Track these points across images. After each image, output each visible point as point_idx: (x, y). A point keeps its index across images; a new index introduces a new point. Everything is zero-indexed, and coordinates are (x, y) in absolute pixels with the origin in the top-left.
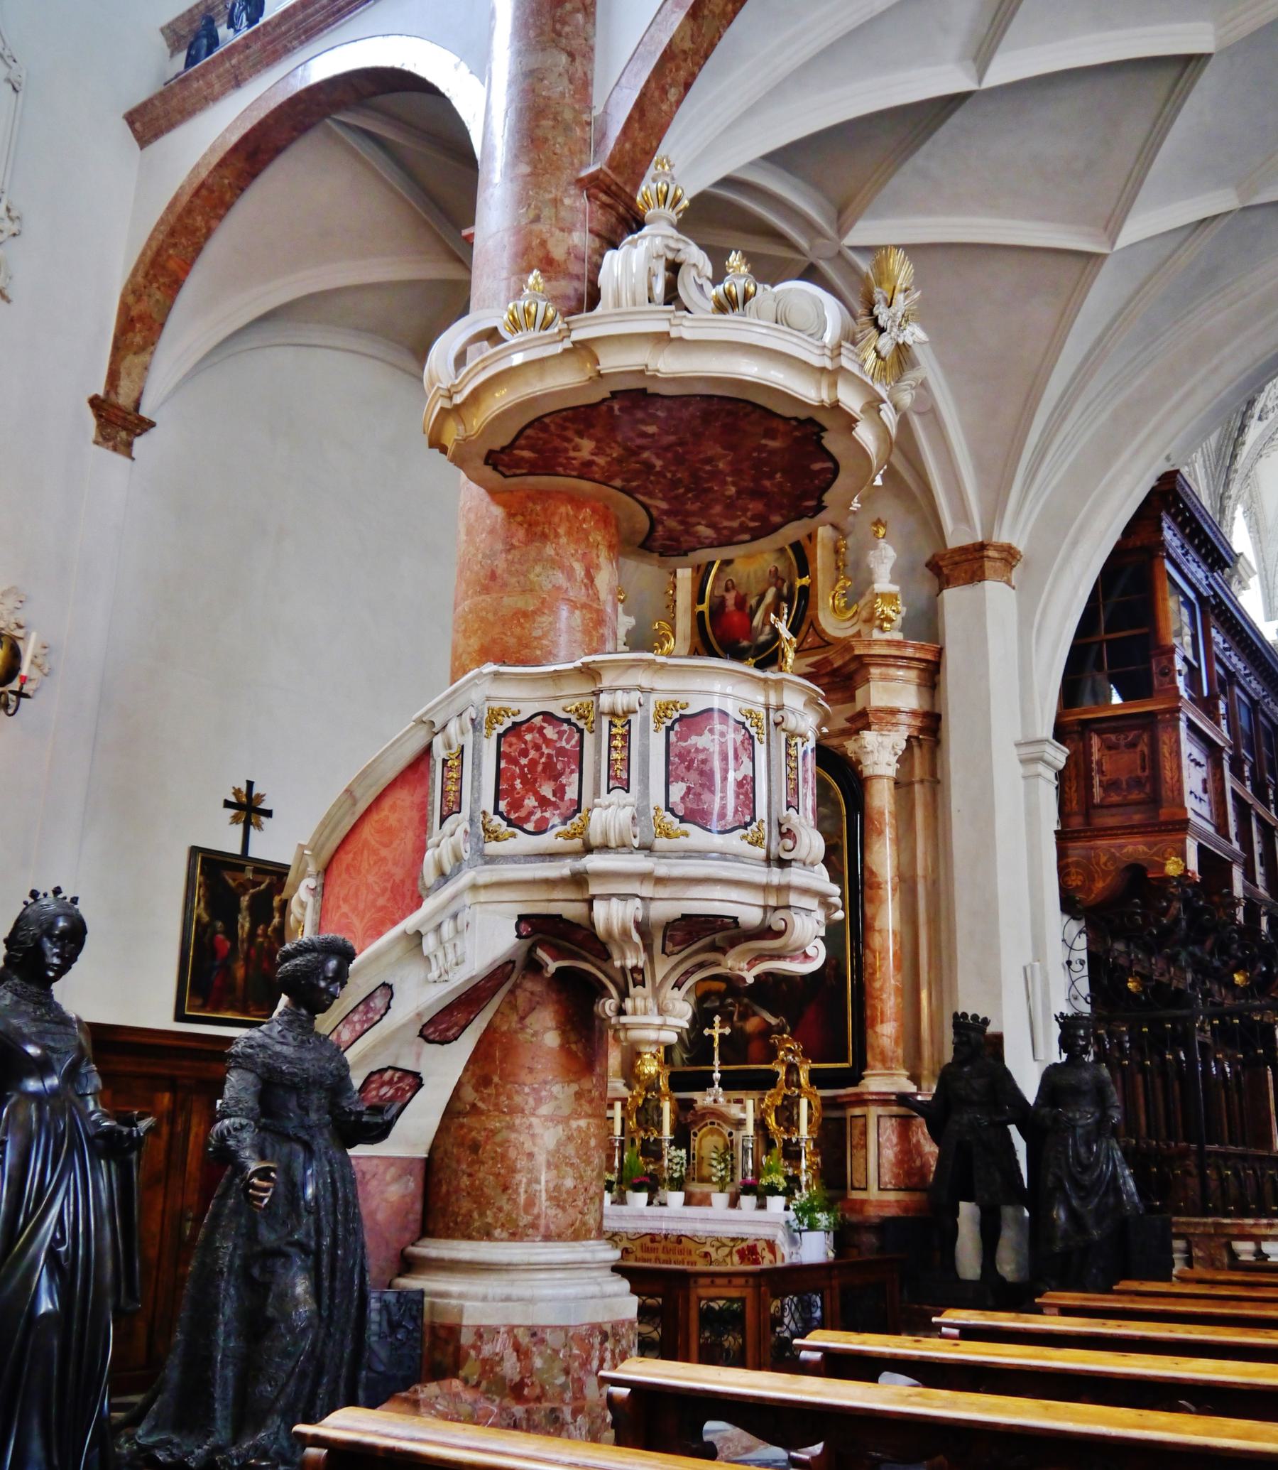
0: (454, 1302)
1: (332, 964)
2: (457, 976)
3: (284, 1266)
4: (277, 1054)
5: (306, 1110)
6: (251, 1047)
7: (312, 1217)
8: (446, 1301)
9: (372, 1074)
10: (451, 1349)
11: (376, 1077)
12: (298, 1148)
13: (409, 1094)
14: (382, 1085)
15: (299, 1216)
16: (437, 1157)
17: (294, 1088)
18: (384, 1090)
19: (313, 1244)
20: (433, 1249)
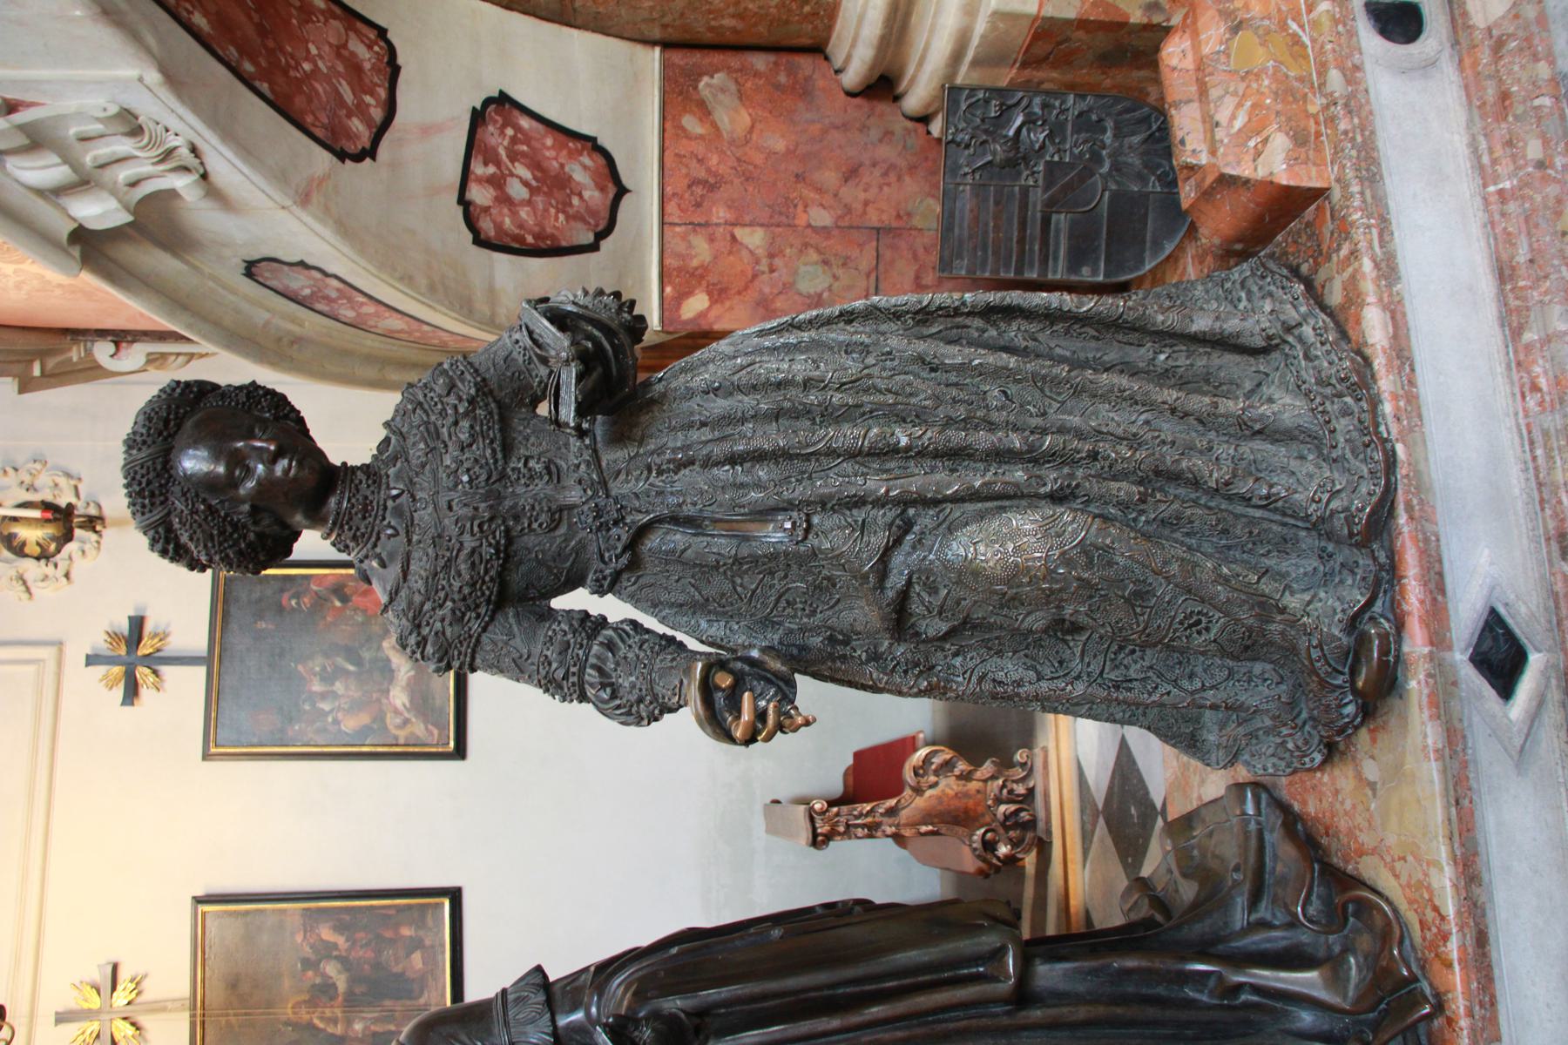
0: (980, 27)
1: (194, 462)
2: (174, 124)
3: (933, 591)
4: (430, 592)
5: (559, 513)
6: (422, 643)
7: (816, 520)
8: (975, 41)
9: (480, 241)
10: (1080, 34)
11: (486, 226)
12: (653, 542)
13: (525, 123)
14: (504, 199)
15: (814, 553)
16: (657, 33)
17: (507, 553)
18: (517, 190)
19: (883, 516)
20: (856, 50)
